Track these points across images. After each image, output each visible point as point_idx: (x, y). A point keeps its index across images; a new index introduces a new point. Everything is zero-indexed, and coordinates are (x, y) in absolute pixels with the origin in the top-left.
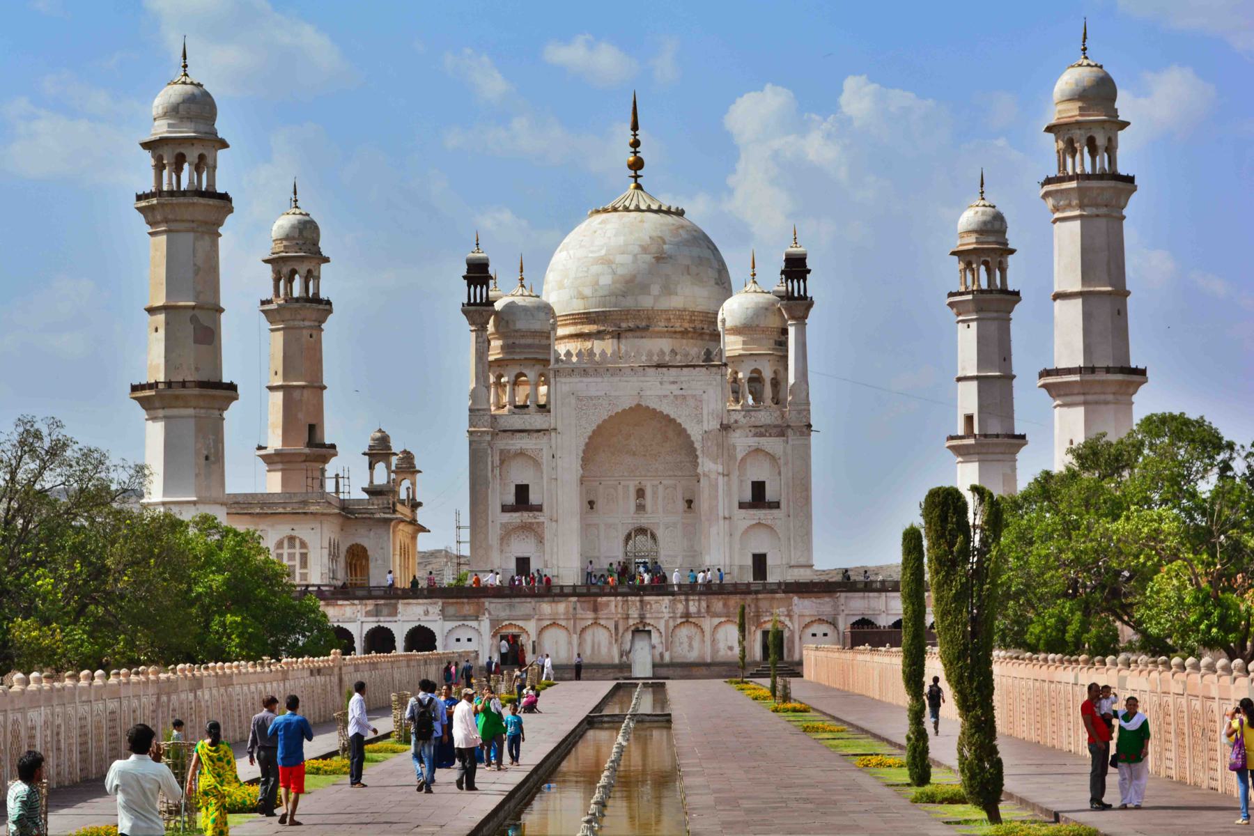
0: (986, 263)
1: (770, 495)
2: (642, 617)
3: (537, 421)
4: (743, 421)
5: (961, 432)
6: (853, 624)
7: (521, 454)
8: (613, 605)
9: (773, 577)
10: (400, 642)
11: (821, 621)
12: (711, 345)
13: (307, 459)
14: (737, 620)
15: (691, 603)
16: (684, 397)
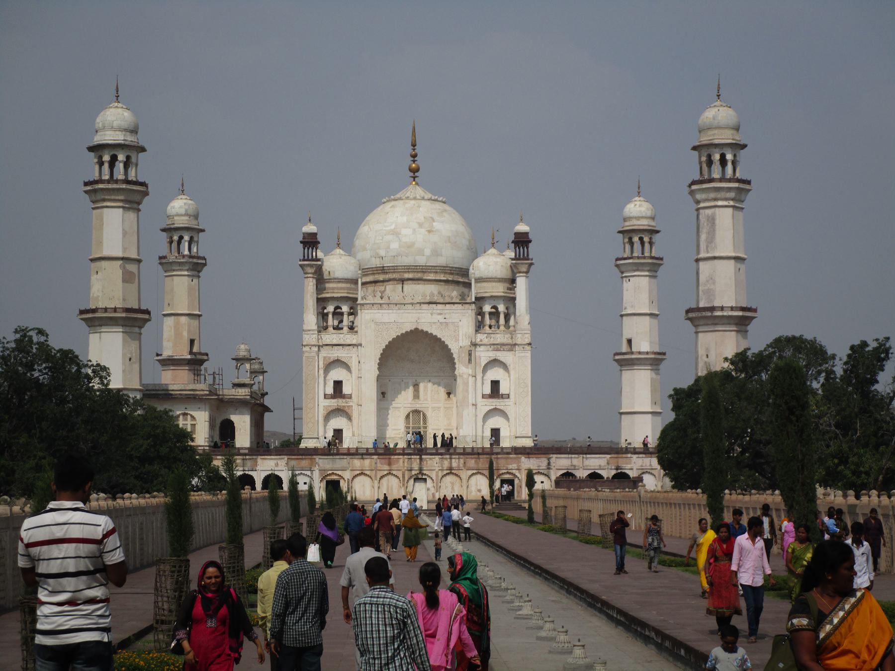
0: (641, 239)
1: (503, 390)
2: (421, 470)
3: (350, 338)
4: (486, 341)
5: (624, 350)
6: (563, 475)
8: (401, 461)
9: (505, 443)
10: (259, 486)
11: (539, 473)
12: (466, 290)
13: (189, 362)
14: (487, 473)
15: (453, 460)
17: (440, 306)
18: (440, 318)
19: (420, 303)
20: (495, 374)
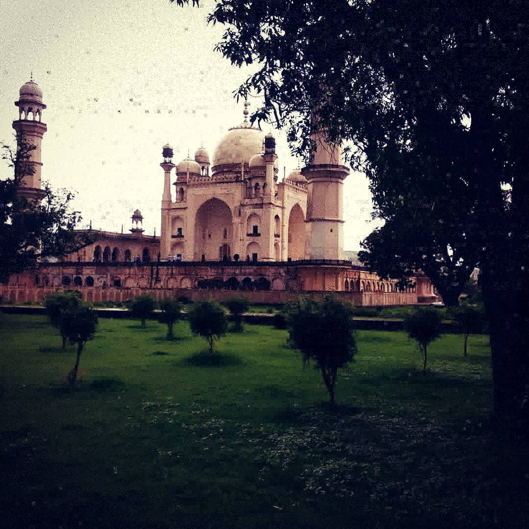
7: (178, 218)
16: (228, 194)
17: (225, 184)
18: (225, 191)
19: (216, 183)
20: (254, 223)
